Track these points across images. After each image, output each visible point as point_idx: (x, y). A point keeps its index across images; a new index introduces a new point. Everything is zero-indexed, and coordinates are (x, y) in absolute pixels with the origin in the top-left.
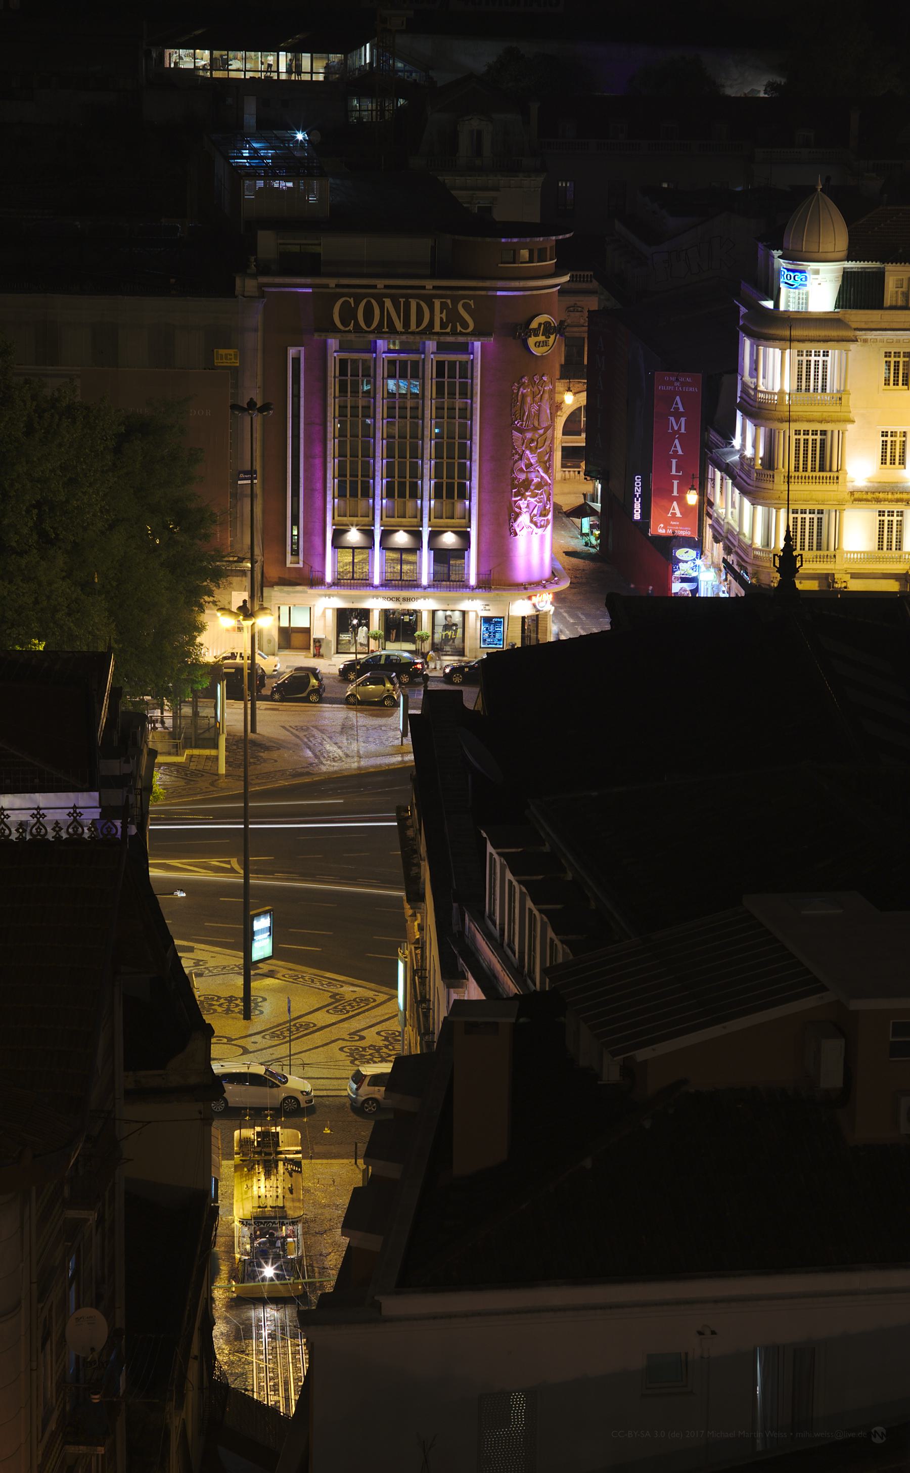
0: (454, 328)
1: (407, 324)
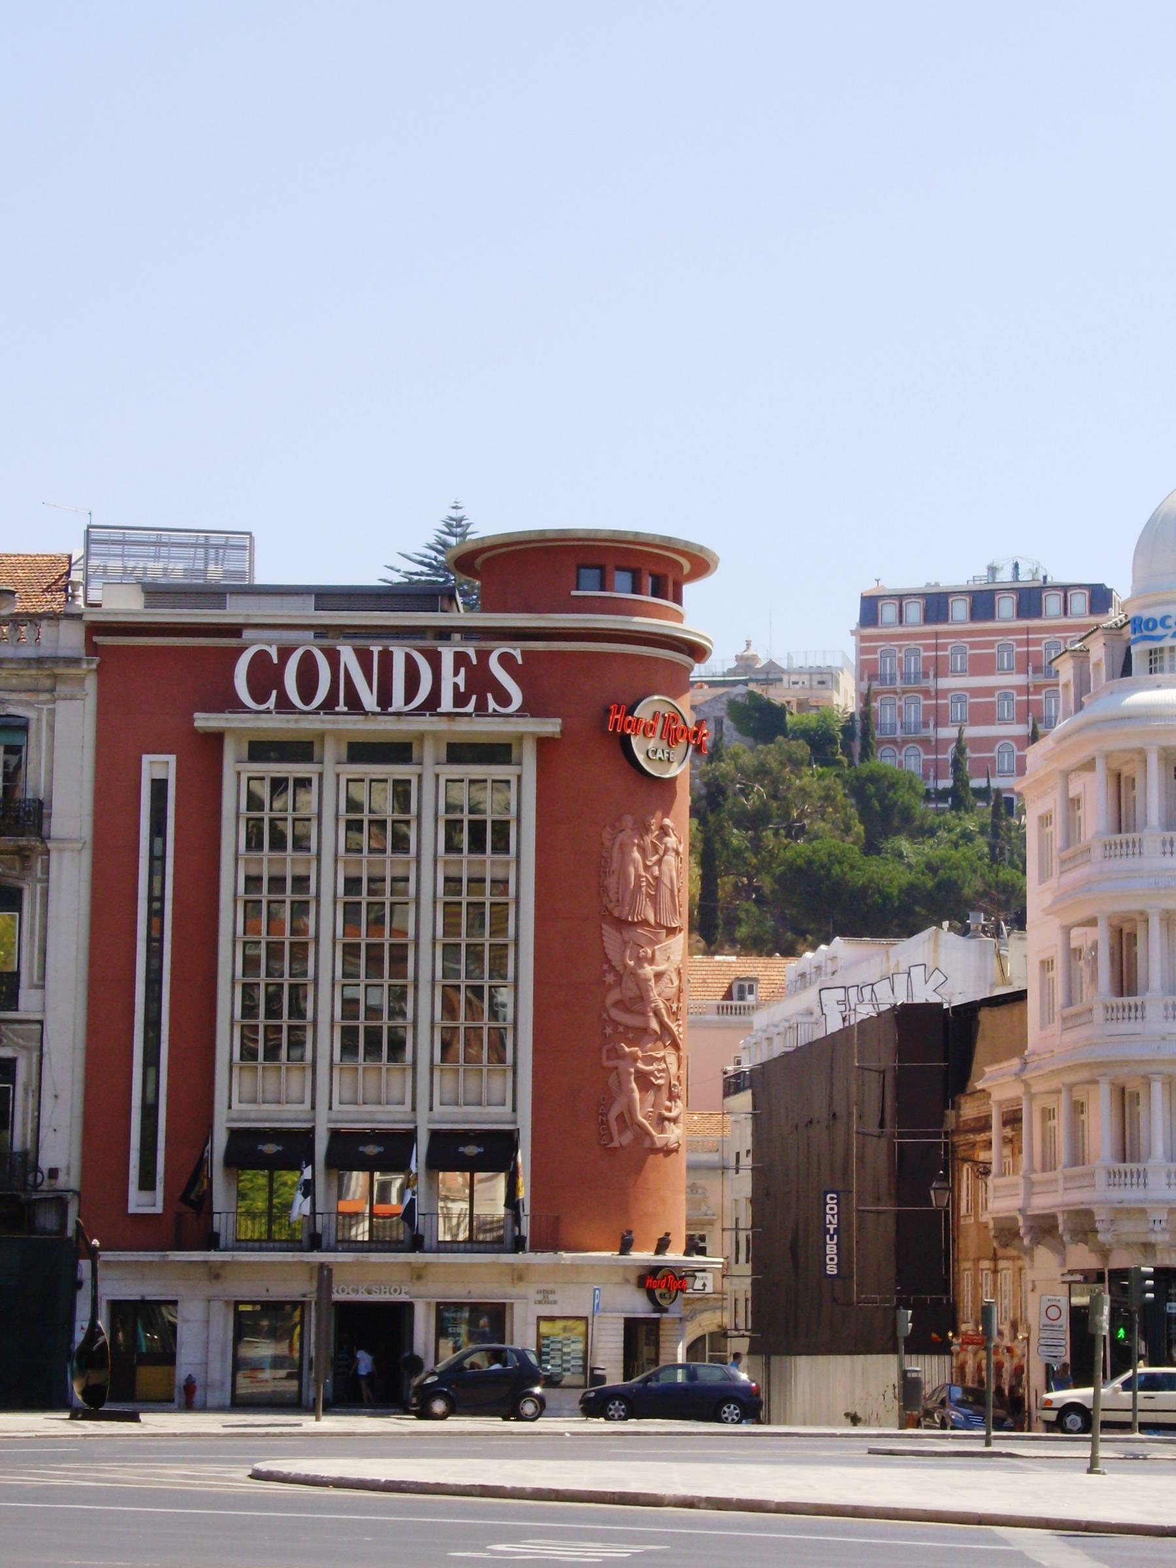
0: (481, 708)
1: (385, 699)
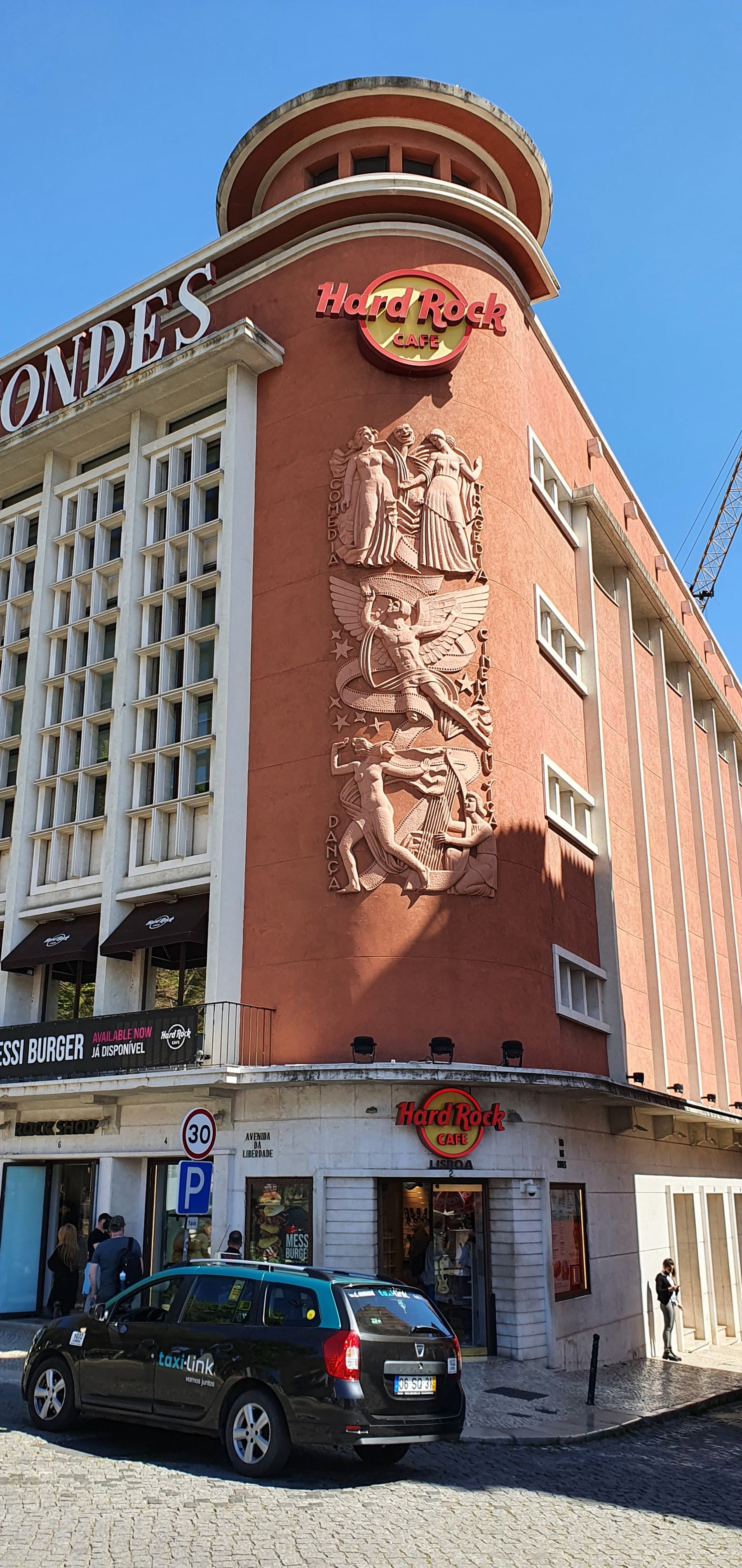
0: (170, 348)
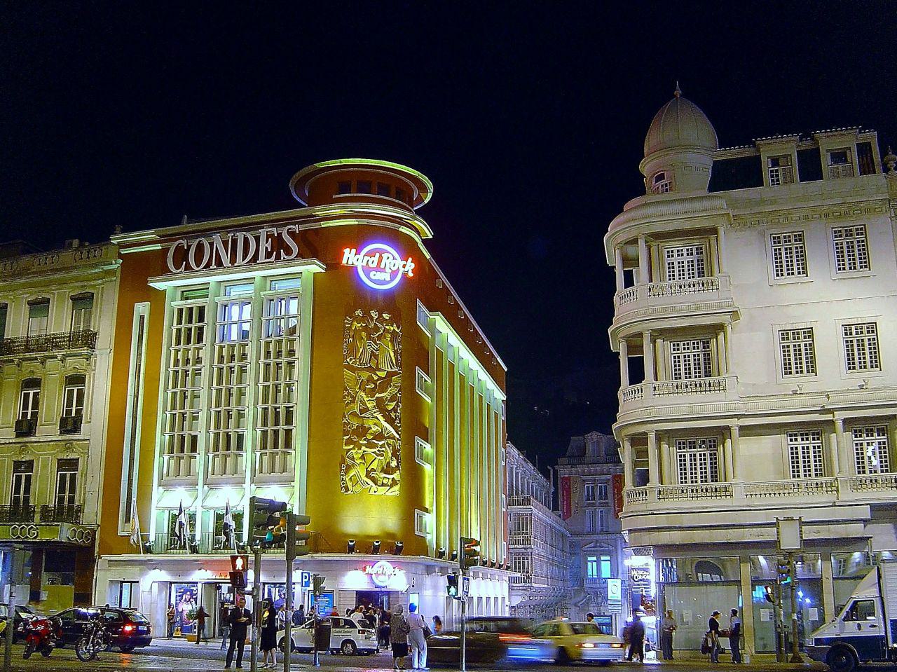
0: (278, 257)
1: (233, 261)
